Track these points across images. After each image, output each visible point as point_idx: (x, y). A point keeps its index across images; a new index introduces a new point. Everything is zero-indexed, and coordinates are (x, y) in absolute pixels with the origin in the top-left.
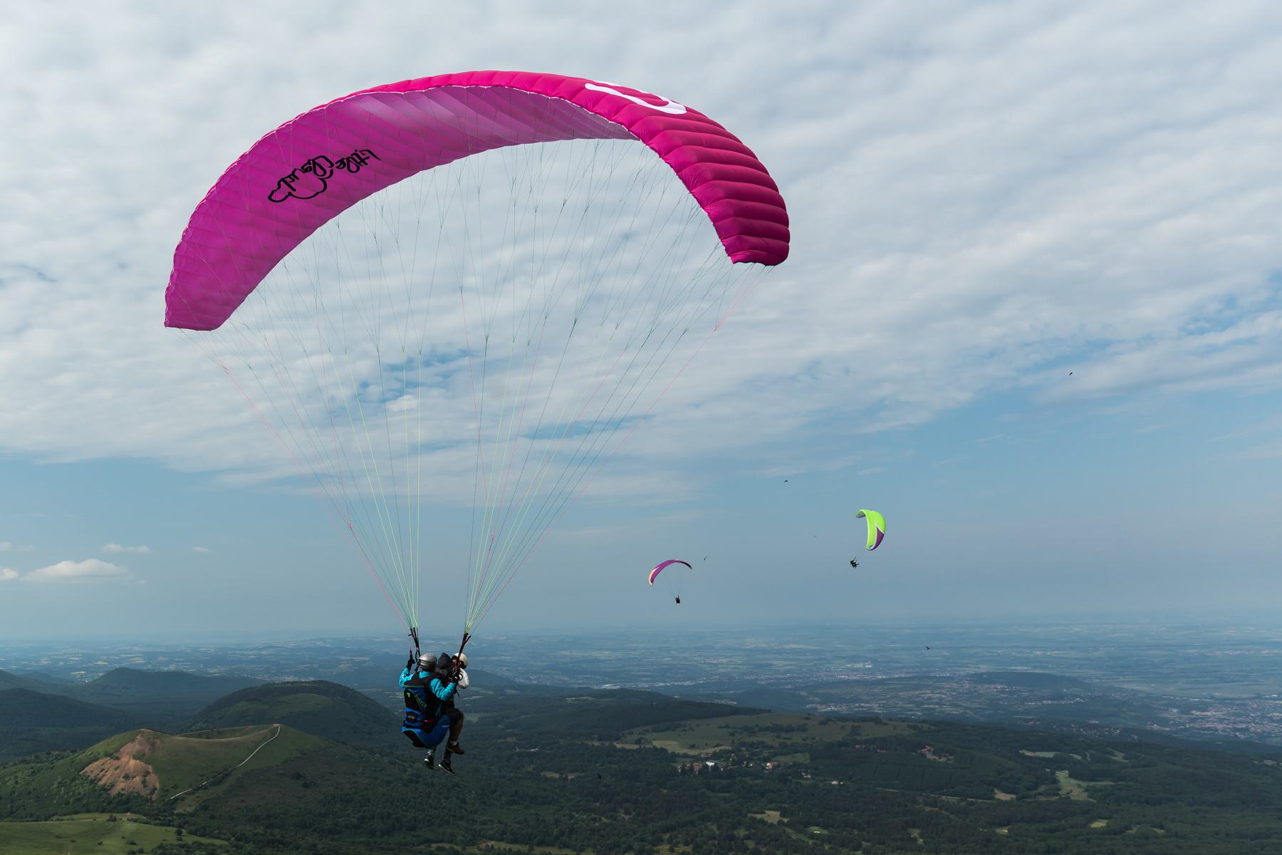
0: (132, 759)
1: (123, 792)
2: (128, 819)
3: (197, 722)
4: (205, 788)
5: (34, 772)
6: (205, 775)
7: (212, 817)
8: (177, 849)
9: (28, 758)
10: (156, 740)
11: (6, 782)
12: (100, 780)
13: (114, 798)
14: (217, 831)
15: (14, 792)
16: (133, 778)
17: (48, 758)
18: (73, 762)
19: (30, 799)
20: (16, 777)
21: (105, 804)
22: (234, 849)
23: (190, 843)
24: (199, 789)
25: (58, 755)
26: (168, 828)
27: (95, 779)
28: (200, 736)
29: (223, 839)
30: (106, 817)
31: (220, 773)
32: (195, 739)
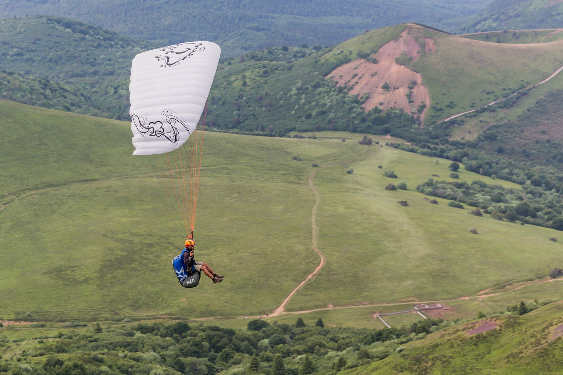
0: (394, 63)
1: (380, 108)
2: (387, 144)
3: (485, 20)
4: (492, 110)
5: (266, 72)
6: (493, 92)
7: (500, 151)
8: (452, 189)
9: (259, 53)
10: (428, 40)
11: (232, 82)
12: (351, 88)
13: (369, 114)
14: (507, 170)
15: (241, 97)
16: (395, 89)
17: (284, 55)
18: (316, 62)
19: (261, 106)
20: (244, 77)
21: (356, 122)
22: (530, 196)
23: (469, 183)
24: (484, 110)
25: (297, 52)
26: (441, 161)
27: (345, 88)
28: (487, 38)
29: (514, 182)
30: (359, 137)
31: (513, 93)
32: (481, 42)
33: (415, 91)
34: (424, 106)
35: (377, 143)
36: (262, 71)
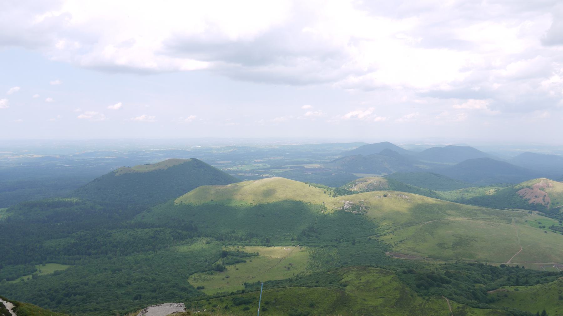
1: (535, 202)
12: (525, 196)
13: (530, 204)
16: (539, 197)
18: (513, 188)
27: (522, 196)
33: (546, 198)
34: (549, 203)
35: (534, 213)
36: (495, 190)
